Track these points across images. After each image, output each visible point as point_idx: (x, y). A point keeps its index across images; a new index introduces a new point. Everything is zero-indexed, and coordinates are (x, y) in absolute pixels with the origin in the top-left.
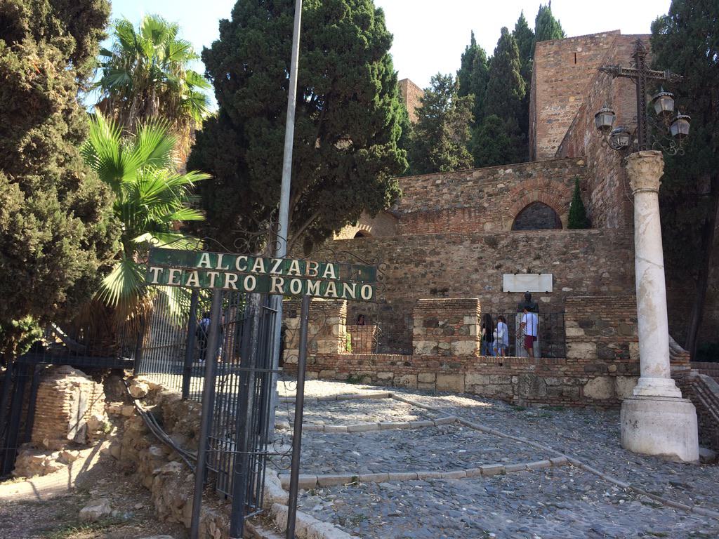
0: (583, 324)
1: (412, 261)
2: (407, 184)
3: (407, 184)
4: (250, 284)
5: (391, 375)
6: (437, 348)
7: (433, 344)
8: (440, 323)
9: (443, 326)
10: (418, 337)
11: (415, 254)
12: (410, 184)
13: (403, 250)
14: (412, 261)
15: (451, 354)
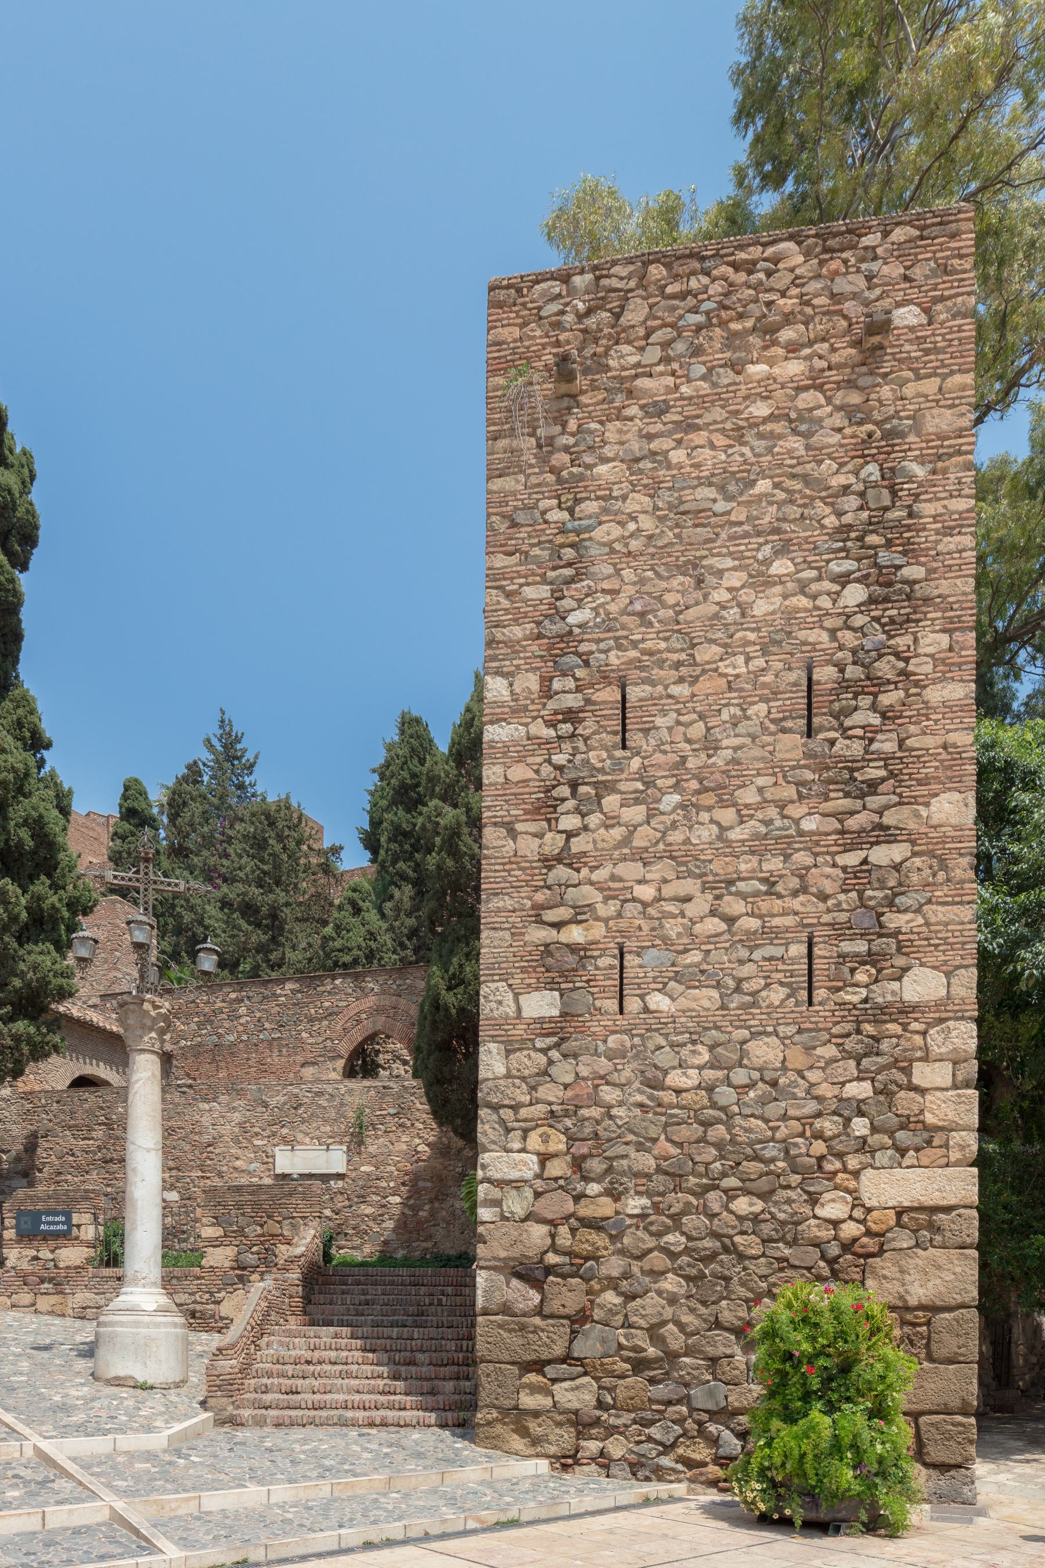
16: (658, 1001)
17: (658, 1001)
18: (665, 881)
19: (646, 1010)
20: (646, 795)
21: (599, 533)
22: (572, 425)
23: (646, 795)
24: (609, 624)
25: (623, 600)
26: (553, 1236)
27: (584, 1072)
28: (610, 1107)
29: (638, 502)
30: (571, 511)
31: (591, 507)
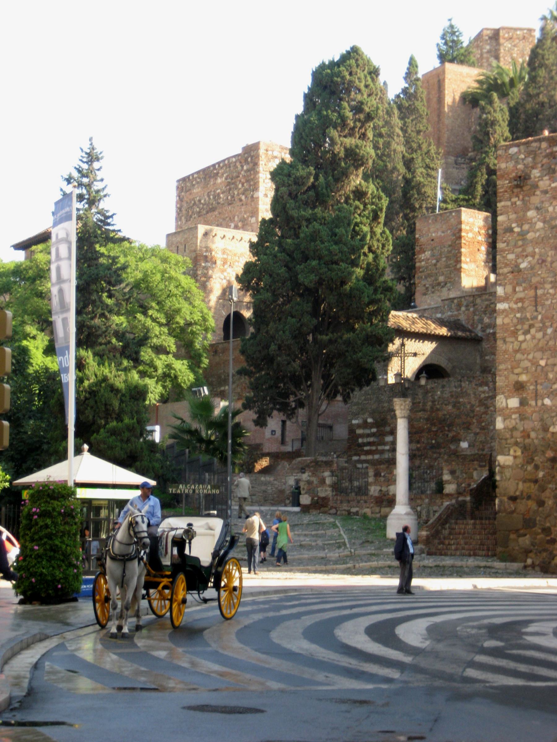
0: (452, 472)
1: (449, 403)
2: (487, 300)
3: (487, 300)
4: (191, 492)
5: (357, 509)
6: (381, 491)
7: (378, 488)
8: (382, 474)
9: (384, 476)
10: (371, 484)
11: (452, 396)
12: (490, 300)
13: (442, 392)
14: (449, 403)
15: (388, 494)
16: (547, 402)
17: (547, 402)
18: (548, 359)
19: (543, 404)
20: (543, 329)
21: (530, 236)
22: (521, 197)
23: (543, 329)
24: (532, 268)
25: (535, 260)
26: (518, 484)
27: (526, 427)
28: (533, 439)
29: (540, 225)
30: (521, 227)
31: (526, 227)
